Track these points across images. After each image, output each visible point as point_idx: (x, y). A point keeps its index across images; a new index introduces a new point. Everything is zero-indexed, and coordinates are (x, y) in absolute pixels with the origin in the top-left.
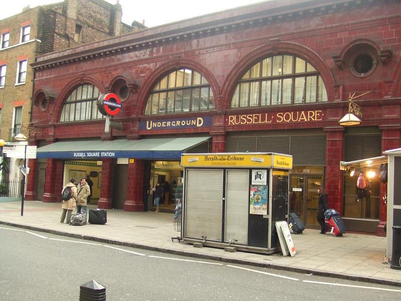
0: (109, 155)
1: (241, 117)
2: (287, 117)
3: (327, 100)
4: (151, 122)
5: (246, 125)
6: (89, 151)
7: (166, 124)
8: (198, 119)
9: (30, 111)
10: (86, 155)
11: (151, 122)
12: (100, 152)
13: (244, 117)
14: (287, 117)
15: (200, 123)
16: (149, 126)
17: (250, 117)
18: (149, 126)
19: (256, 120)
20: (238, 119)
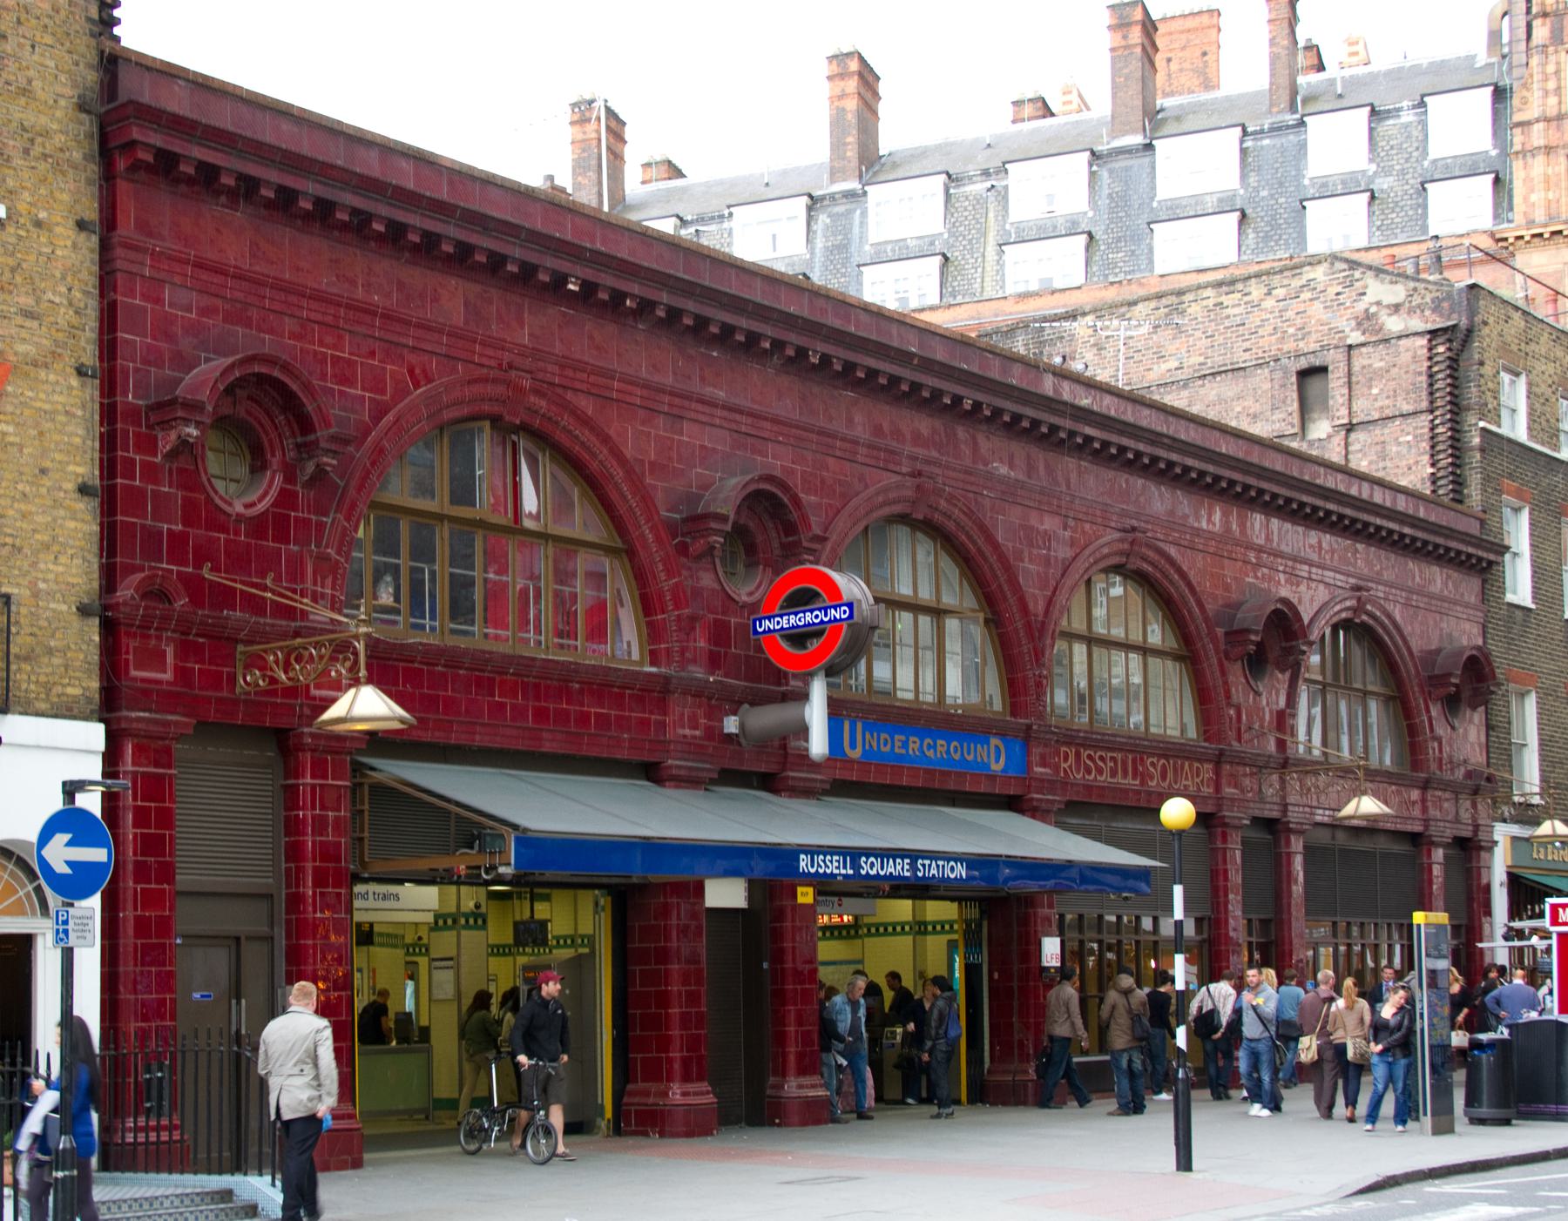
0: (947, 871)
1: (1085, 754)
2: (1164, 777)
3: (1192, 733)
4: (859, 725)
5: (1089, 788)
6: (869, 852)
7: (905, 744)
8: (994, 741)
9: (85, 467)
10: (856, 866)
11: (859, 725)
12: (914, 856)
13: (1090, 757)
14: (1164, 777)
15: (997, 761)
16: (853, 745)
17: (1101, 758)
18: (853, 745)
19: (1114, 773)
20: (1078, 755)
